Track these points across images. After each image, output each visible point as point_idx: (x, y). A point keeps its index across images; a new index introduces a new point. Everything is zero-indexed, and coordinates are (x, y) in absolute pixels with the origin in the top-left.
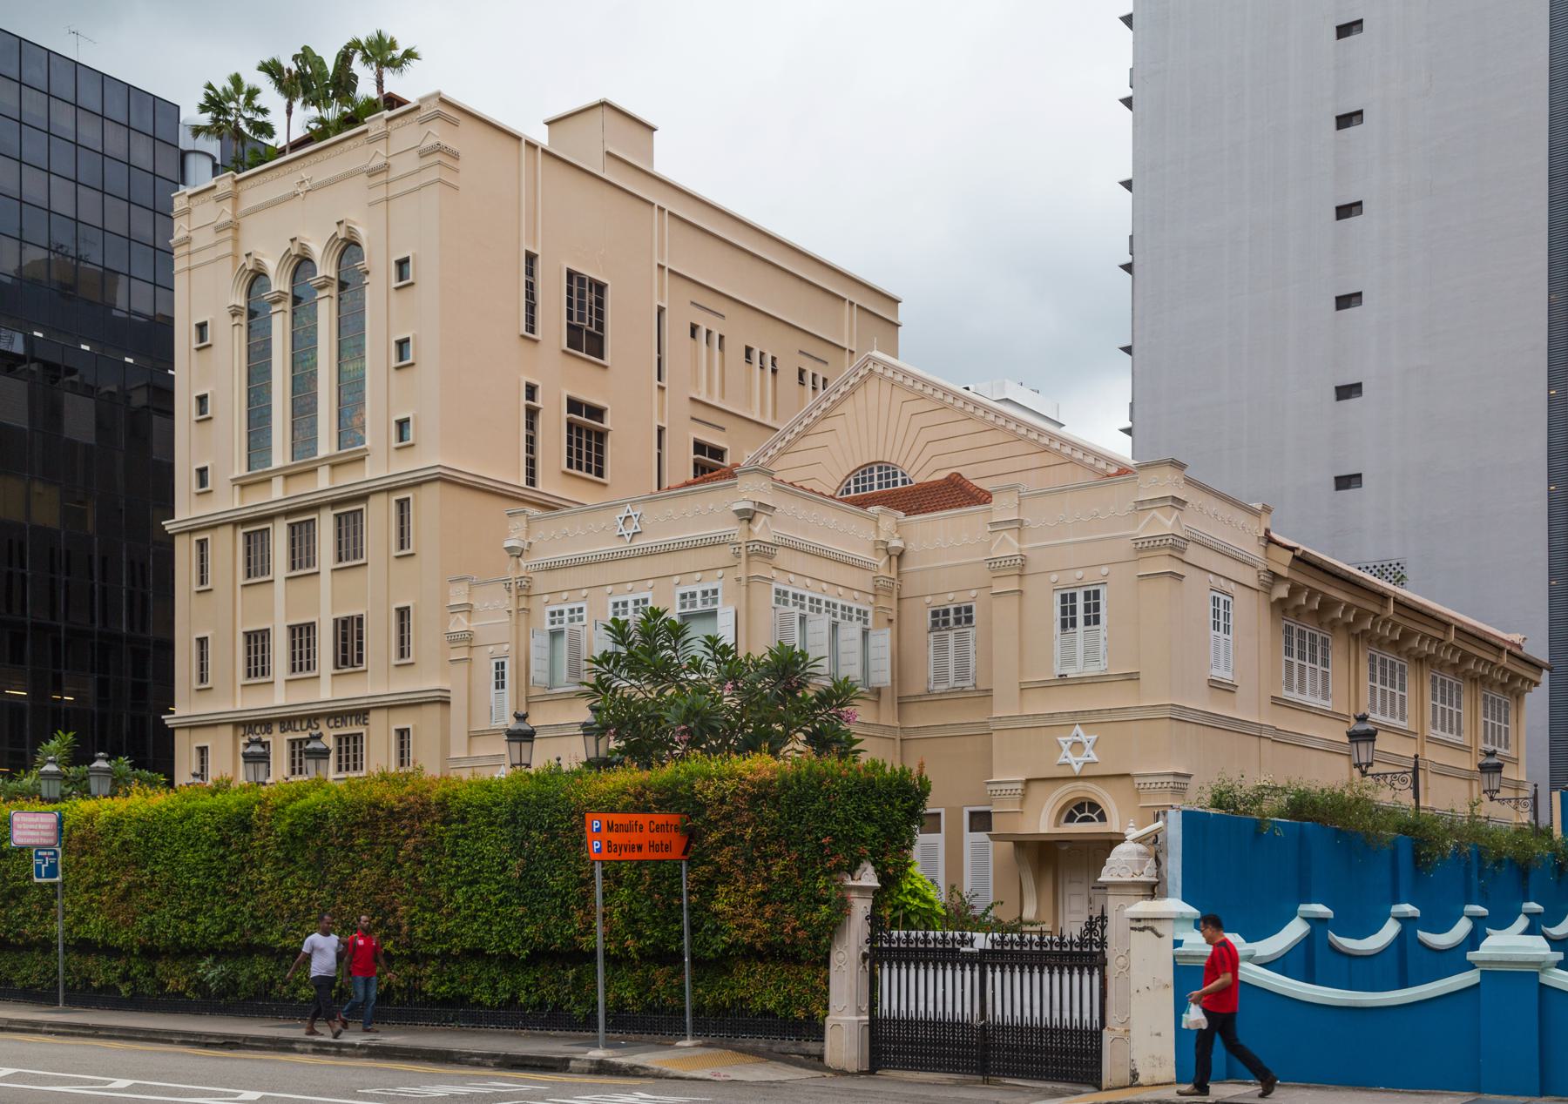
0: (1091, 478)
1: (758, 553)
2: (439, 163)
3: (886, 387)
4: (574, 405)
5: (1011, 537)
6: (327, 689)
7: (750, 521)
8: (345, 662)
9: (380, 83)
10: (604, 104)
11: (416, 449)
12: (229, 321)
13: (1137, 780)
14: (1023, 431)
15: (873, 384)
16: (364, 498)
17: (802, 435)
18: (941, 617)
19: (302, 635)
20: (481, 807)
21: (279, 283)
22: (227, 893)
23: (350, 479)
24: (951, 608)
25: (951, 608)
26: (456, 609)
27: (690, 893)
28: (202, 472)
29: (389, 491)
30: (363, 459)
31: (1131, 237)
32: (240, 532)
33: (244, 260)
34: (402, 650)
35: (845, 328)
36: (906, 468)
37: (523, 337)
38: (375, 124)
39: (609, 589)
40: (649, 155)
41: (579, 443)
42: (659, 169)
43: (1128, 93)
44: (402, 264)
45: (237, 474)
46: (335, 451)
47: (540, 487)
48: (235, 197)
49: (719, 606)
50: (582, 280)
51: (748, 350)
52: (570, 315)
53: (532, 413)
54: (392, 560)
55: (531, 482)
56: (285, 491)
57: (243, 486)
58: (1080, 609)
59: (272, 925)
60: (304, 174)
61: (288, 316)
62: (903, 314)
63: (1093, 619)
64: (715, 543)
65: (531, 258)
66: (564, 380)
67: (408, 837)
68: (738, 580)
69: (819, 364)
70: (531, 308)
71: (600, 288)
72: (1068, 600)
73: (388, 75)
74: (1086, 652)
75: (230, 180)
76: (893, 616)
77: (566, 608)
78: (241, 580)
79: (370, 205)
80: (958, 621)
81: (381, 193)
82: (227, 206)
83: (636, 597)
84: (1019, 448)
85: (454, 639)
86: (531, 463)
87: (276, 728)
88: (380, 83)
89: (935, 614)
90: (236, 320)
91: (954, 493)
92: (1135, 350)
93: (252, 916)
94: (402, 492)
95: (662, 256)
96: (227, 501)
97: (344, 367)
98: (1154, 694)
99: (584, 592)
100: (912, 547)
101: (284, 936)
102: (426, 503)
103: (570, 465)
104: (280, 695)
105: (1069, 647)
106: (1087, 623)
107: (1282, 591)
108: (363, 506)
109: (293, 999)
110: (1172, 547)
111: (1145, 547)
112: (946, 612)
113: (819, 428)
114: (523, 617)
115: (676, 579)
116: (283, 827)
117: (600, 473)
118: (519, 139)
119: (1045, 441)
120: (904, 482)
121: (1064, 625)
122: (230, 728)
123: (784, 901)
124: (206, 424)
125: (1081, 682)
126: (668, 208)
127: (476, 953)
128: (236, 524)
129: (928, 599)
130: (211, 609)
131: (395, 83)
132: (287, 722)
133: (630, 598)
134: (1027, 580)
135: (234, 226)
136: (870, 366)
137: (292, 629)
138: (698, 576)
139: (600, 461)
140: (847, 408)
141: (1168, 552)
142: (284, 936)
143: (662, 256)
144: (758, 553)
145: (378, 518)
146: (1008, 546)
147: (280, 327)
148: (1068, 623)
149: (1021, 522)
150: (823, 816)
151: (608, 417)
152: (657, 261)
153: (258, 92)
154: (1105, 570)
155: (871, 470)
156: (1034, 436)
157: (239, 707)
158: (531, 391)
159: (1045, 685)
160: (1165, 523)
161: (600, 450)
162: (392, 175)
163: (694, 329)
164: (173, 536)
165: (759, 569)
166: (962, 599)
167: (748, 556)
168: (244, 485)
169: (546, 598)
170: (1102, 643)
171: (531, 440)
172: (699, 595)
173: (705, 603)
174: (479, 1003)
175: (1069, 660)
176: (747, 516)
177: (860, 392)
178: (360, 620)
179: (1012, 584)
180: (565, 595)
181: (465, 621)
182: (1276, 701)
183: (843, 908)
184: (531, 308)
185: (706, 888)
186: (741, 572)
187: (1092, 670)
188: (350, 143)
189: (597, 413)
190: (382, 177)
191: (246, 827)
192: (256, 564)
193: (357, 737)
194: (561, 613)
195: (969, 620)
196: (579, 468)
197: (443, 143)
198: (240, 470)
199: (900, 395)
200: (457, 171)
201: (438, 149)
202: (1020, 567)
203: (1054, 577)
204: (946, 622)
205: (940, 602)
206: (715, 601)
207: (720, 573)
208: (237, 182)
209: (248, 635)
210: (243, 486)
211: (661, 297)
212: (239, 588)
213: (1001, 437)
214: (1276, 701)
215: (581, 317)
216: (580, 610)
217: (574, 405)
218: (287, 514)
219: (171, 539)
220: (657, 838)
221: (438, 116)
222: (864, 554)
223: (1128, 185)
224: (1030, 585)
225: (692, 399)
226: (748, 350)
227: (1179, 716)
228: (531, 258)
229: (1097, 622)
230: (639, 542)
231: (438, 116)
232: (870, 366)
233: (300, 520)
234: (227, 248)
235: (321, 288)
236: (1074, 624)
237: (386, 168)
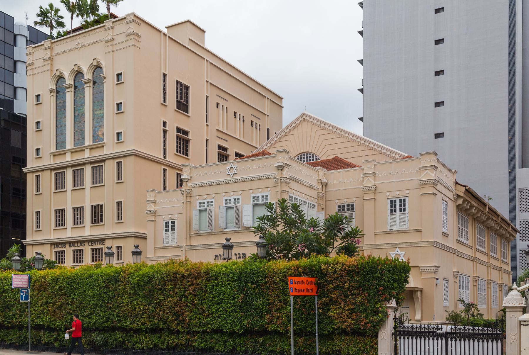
0: (389, 160)
1: (285, 182)
2: (134, 39)
3: (310, 125)
4: (179, 130)
5: (371, 179)
6: (88, 231)
7: (282, 170)
8: (95, 221)
9: (109, 9)
10: (188, 21)
11: (124, 143)
12: (49, 94)
13: (421, 268)
14: (363, 142)
15: (305, 123)
16: (103, 161)
17: (277, 142)
18: (342, 208)
19: (78, 211)
20: (224, 274)
21: (69, 80)
22: (106, 307)
23: (98, 154)
24: (346, 205)
25: (346, 205)
26: (150, 202)
27: (318, 308)
28: (38, 150)
29: (114, 158)
30: (103, 147)
31: (362, 80)
33: (55, 72)
34: (118, 217)
35: (266, 107)
36: (318, 154)
37: (162, 104)
38: (108, 23)
39: (224, 194)
40: (203, 41)
41: (180, 144)
42: (207, 46)
43: (361, 29)
44: (119, 75)
45: (52, 151)
46: (91, 143)
47: (167, 159)
48: (51, 48)
50: (181, 85)
51: (235, 113)
52: (177, 98)
53: (165, 132)
54: (115, 184)
55: (164, 157)
56: (72, 158)
58: (398, 205)
59: (126, 319)
60: (79, 41)
61: (73, 93)
62: (284, 103)
63: (402, 209)
65: (164, 75)
66: (176, 121)
67: (190, 286)
68: (277, 192)
69: (258, 119)
70: (164, 94)
71: (187, 88)
72: (393, 203)
73: (112, 6)
74: (400, 221)
75: (49, 42)
76: (324, 207)
77: (206, 201)
78: (53, 190)
79: (106, 53)
80: (348, 209)
81: (110, 49)
82: (48, 52)
84: (361, 148)
85: (149, 213)
86: (164, 150)
87: (67, 246)
88: (109, 9)
89: (339, 207)
90: (52, 94)
91: (336, 164)
92: (364, 119)
93: (117, 316)
94: (119, 160)
95: (207, 78)
96: (48, 161)
97: (95, 113)
98: (427, 237)
99: (214, 195)
100: (330, 182)
101: (131, 324)
102: (128, 164)
103: (177, 152)
104: (69, 233)
106: (401, 210)
107: (460, 201)
108: (103, 164)
109: (134, 348)
110: (434, 184)
111: (423, 184)
112: (344, 206)
113: (284, 139)
114: (188, 204)
115: (251, 191)
116: (135, 281)
117: (187, 155)
118: (160, 32)
119: (371, 145)
120: (316, 159)
121: (391, 211)
122: (49, 245)
123: (361, 312)
124: (40, 132)
125: (398, 232)
126: (210, 60)
127: (219, 331)
128: (51, 170)
129: (337, 201)
130: (40, 201)
131: (114, 9)
132: (71, 243)
133: (260, 195)
134: (377, 195)
135: (51, 59)
136: (304, 117)
137: (74, 209)
138: (260, 190)
139: (187, 150)
140: (295, 132)
141: (433, 185)
142: (131, 324)
143: (207, 78)
144: (285, 182)
145: (109, 169)
146: (370, 182)
147: (69, 97)
148: (393, 211)
149: (375, 174)
150: (379, 279)
151: (190, 134)
152: (206, 79)
153: (59, 10)
154: (408, 192)
155: (304, 155)
156: (367, 144)
157: (52, 238)
158: (164, 124)
159: (384, 233)
160: (432, 175)
161: (187, 146)
162: (115, 42)
163: (218, 104)
164: (26, 173)
165: (285, 188)
166: (350, 201)
167: (281, 183)
168: (55, 155)
169: (198, 197)
170: (407, 219)
171: (164, 142)
172: (260, 197)
173: (263, 200)
174: (218, 350)
175: (394, 224)
176: (280, 168)
177: (300, 127)
178: (102, 206)
179: (372, 196)
180: (205, 196)
182: (458, 242)
183: (386, 315)
184: (164, 94)
185: (326, 307)
186: (278, 189)
187: (403, 228)
188: (98, 30)
189: (186, 133)
190: (111, 43)
191: (117, 281)
192: (60, 184)
193: (63, 252)
194: (204, 203)
195: (353, 209)
196: (180, 153)
197: (135, 31)
198: (53, 150)
199: (315, 128)
200: (140, 42)
201: (133, 33)
202: (375, 190)
203: (388, 194)
204: (343, 210)
205: (341, 202)
207: (269, 189)
208: (52, 43)
209: (56, 211)
210: (54, 156)
211: (207, 93)
212: (52, 194)
213: (354, 144)
214: (458, 242)
215: (181, 98)
216: (212, 202)
217: (179, 130)
218: (72, 166)
219: (25, 174)
220: (309, 287)
221: (133, 21)
222: (314, 184)
223: (361, 62)
224: (378, 196)
225: (217, 130)
226: (235, 113)
227: (436, 245)
228: (164, 75)
229: (404, 210)
230: (236, 177)
231: (133, 21)
232: (304, 117)
234: (49, 67)
235: (86, 83)
236: (395, 211)
237: (112, 40)
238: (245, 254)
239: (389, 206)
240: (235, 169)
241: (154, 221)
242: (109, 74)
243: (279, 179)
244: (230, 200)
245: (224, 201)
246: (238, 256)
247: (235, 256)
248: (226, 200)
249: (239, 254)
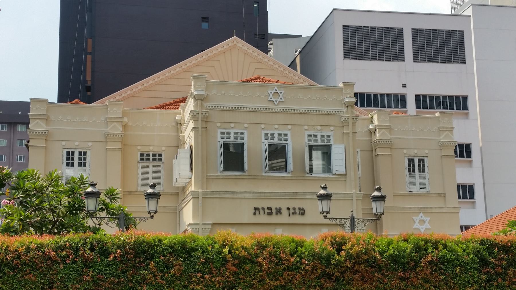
49: (332, 142)
63: (422, 169)
64: (328, 114)
72: (411, 162)
83: (280, 132)
105: (413, 180)
121: (410, 171)
125: (419, 195)
148: (411, 170)
159: (403, 196)
167: (353, 123)
173: (323, 140)
175: (413, 185)
180: (232, 125)
181: (44, 125)
206: (329, 141)
207: (332, 128)
230: (282, 106)
238: (303, 209)
239: (88, 159)
241: (45, 147)
243: (350, 118)
244: (273, 135)
245: (263, 135)
246: (292, 211)
247: (287, 211)
248: (266, 134)
249: (294, 209)
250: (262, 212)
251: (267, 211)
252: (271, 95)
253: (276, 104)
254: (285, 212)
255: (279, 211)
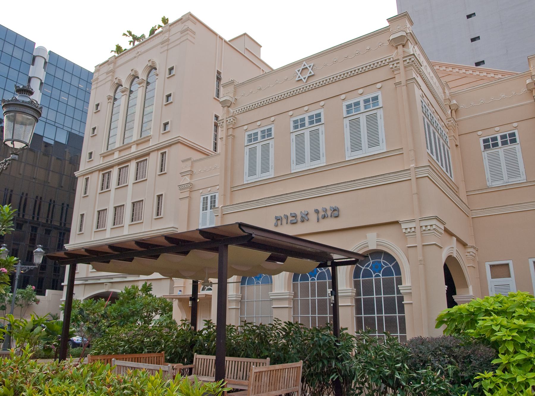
16: (148, 154)
24: (498, 136)
25: (498, 136)
28: (91, 154)
29: (158, 150)
30: (149, 140)
32: (101, 173)
34: (158, 213)
37: (214, 98)
57: (104, 157)
94: (162, 151)
96: (98, 162)
99: (272, 119)
112: (495, 139)
124: (95, 137)
128: (100, 170)
157: (93, 240)
162: (170, 42)
167: (405, 67)
192: (105, 186)
198: (104, 150)
210: (104, 157)
219: (77, 178)
230: (312, 81)
233: (123, 164)
237: (168, 40)
240: (310, 69)
242: (162, 70)
243: (401, 61)
246: (321, 213)
247: (316, 215)
249: (325, 210)
250: (284, 221)
251: (290, 219)
252: (299, 73)
253: (305, 81)
254: (313, 217)
255: (305, 218)
